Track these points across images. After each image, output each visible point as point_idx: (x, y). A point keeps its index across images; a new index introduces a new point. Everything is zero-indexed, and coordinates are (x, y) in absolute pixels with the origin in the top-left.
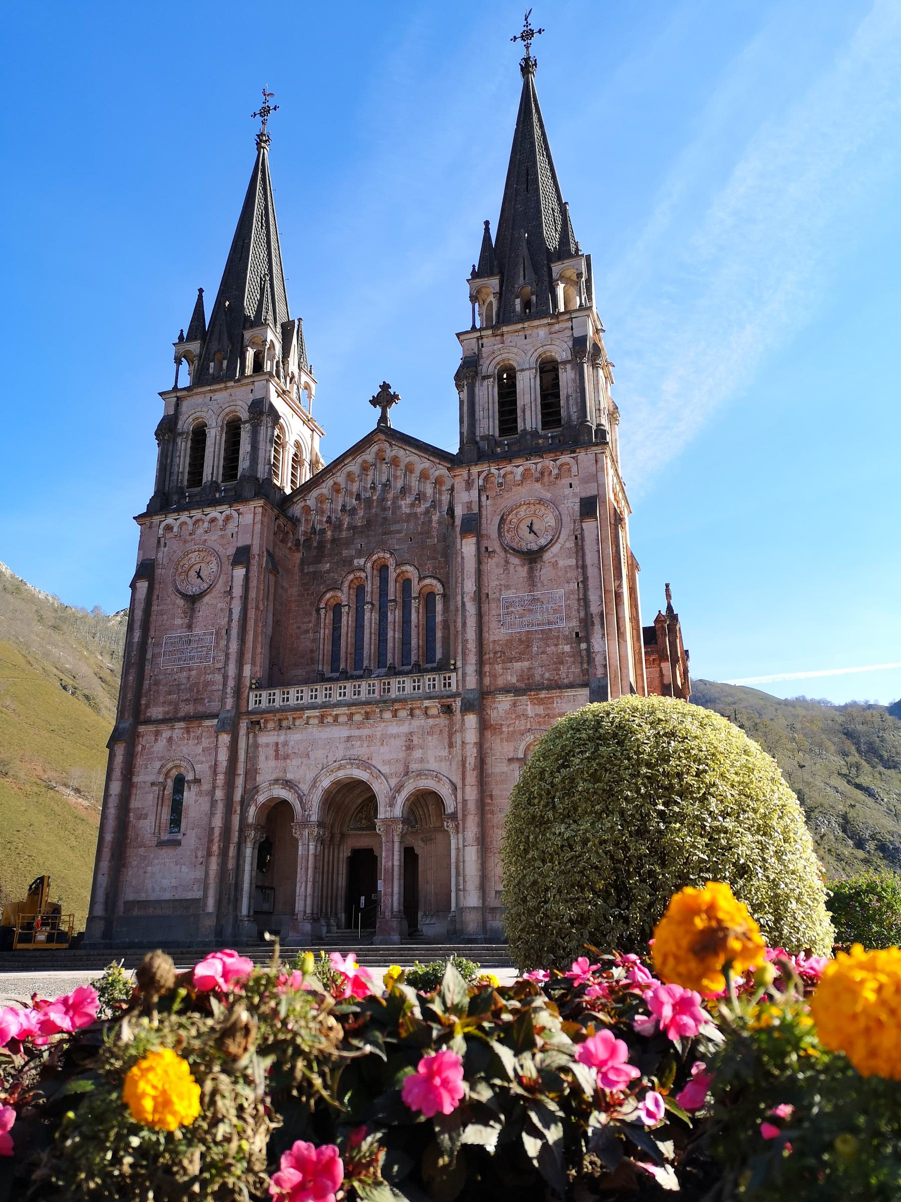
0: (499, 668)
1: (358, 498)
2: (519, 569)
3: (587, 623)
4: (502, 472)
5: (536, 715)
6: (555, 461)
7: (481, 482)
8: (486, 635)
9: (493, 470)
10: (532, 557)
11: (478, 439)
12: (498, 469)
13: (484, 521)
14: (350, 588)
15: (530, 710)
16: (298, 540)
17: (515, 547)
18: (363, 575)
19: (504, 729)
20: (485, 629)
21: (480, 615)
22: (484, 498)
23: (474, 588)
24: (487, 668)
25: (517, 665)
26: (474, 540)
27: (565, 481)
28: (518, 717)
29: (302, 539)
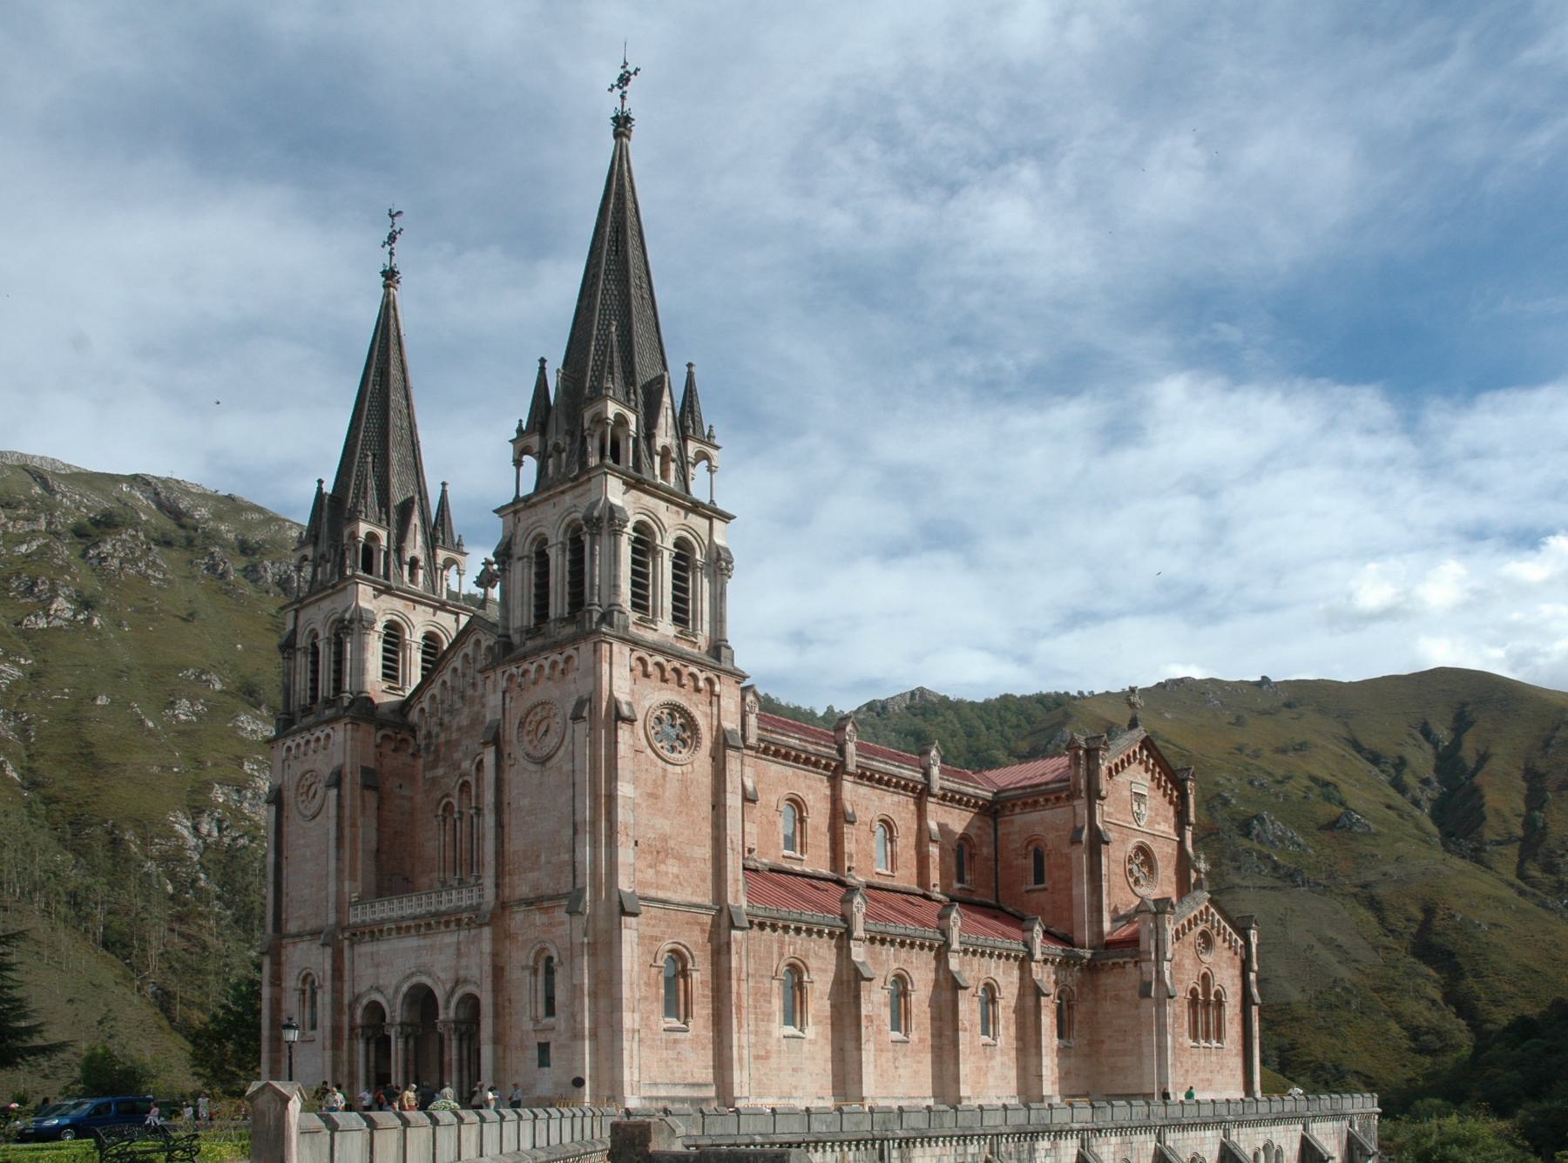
0: (516, 878)
1: (463, 697)
2: (533, 776)
3: (575, 832)
4: (521, 670)
5: (543, 924)
6: (561, 654)
7: (504, 684)
8: (506, 846)
9: (514, 670)
10: (543, 761)
11: (511, 632)
12: (518, 668)
13: (507, 726)
14: (461, 791)
15: (539, 918)
16: (419, 745)
17: (532, 753)
18: (466, 778)
19: (520, 938)
20: (506, 840)
21: (500, 826)
22: (507, 701)
23: (493, 800)
24: (507, 879)
25: (531, 875)
26: (493, 749)
27: (570, 676)
28: (530, 926)
29: (423, 743)
